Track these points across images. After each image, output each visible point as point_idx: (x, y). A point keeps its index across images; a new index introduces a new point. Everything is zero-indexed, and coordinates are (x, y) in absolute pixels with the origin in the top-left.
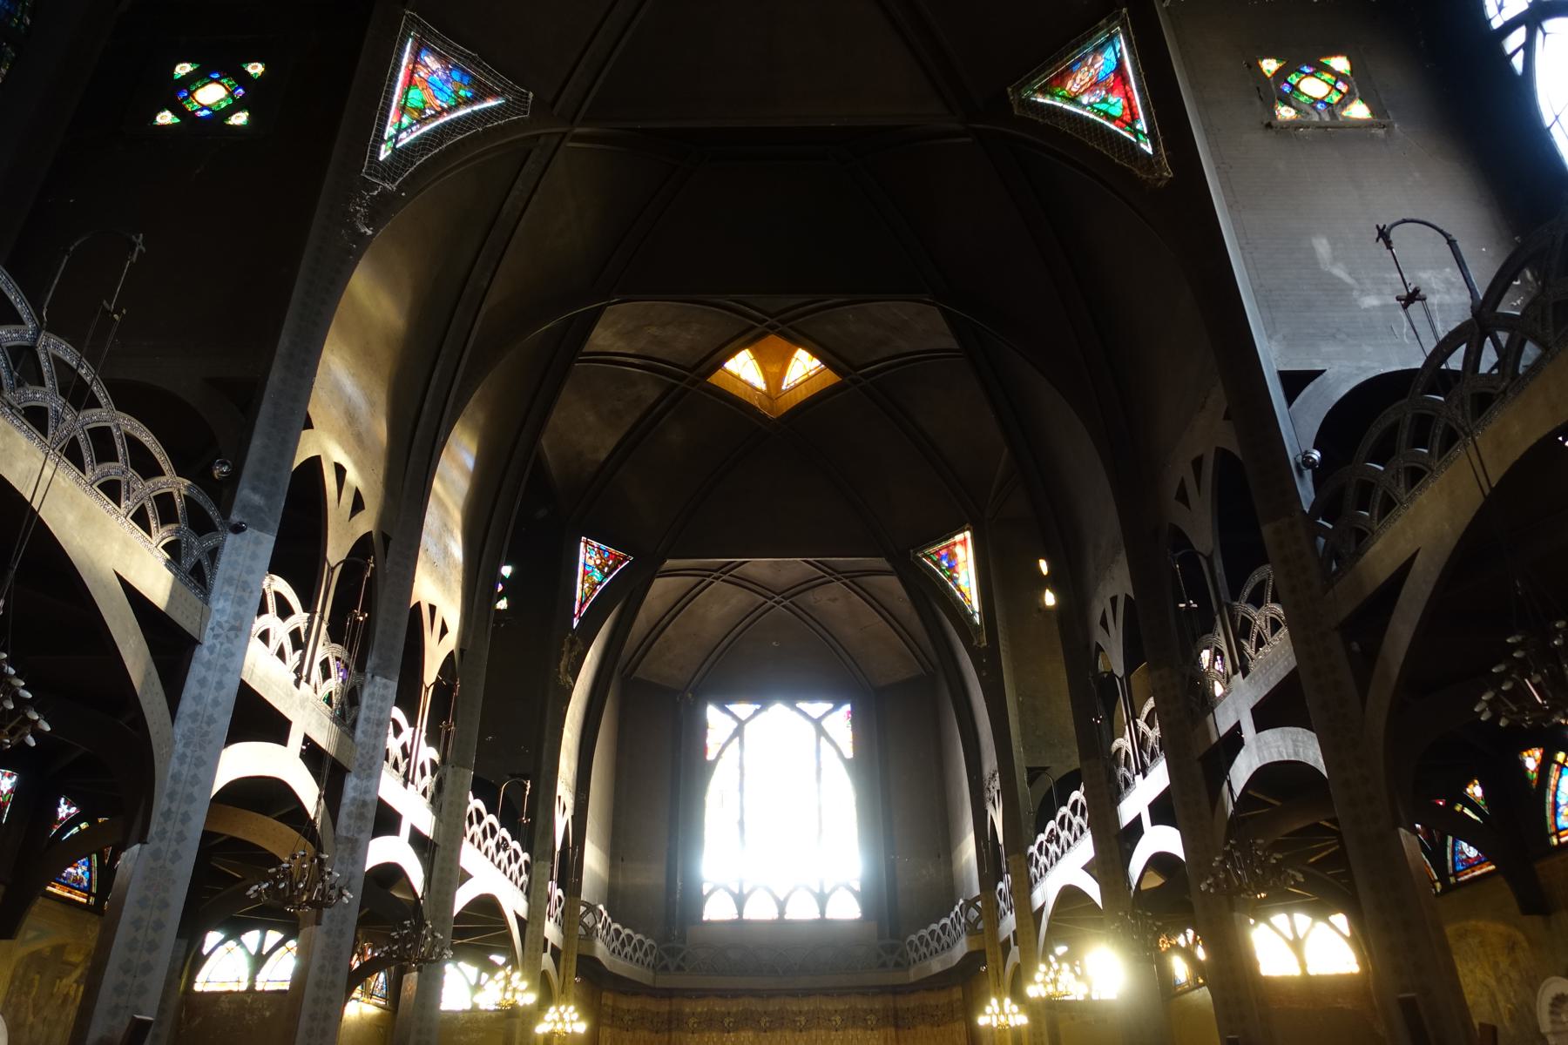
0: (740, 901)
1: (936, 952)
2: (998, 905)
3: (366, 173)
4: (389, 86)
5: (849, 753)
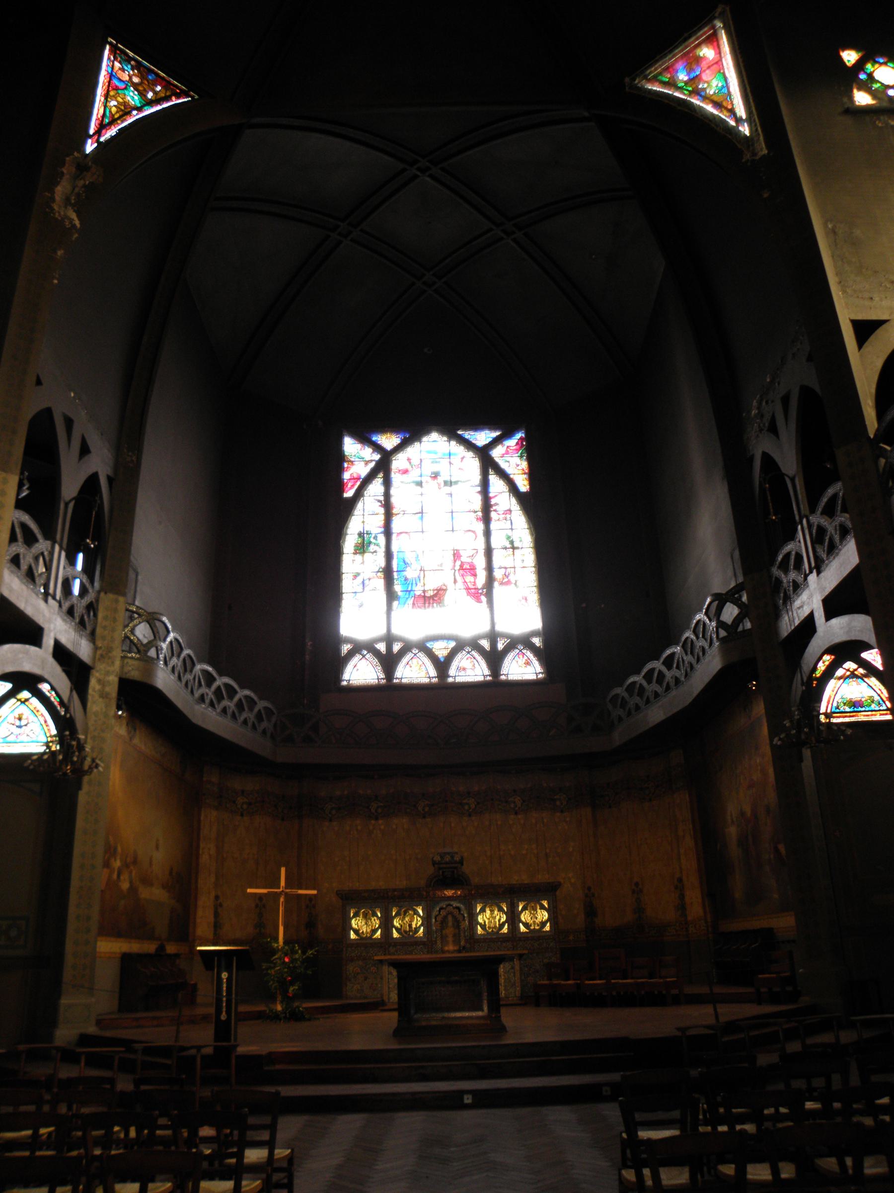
0: (389, 662)
1: (657, 695)
2: (779, 582)
5: (523, 485)
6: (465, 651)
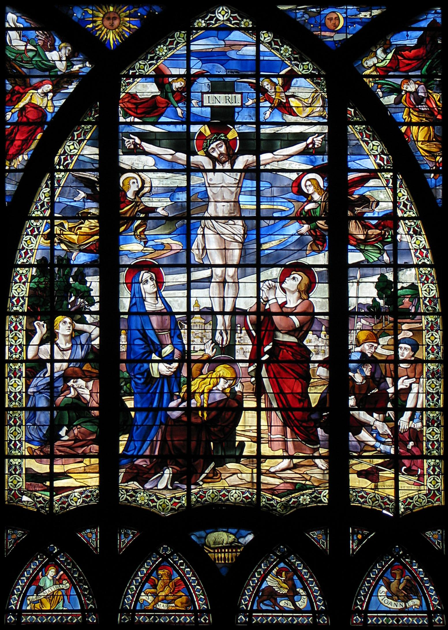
6: (275, 554)
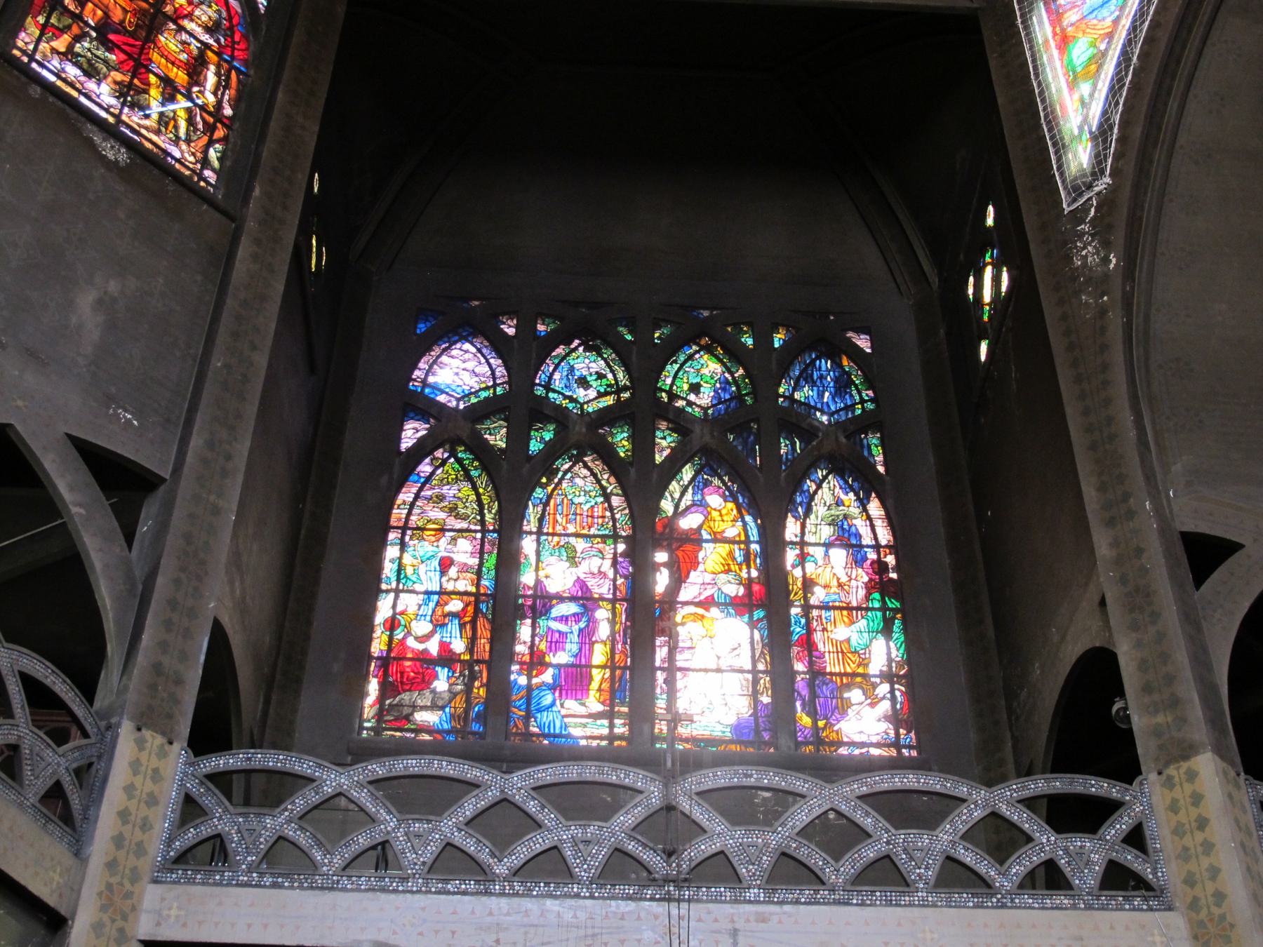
3: (1069, 205)
4: (1039, 84)
